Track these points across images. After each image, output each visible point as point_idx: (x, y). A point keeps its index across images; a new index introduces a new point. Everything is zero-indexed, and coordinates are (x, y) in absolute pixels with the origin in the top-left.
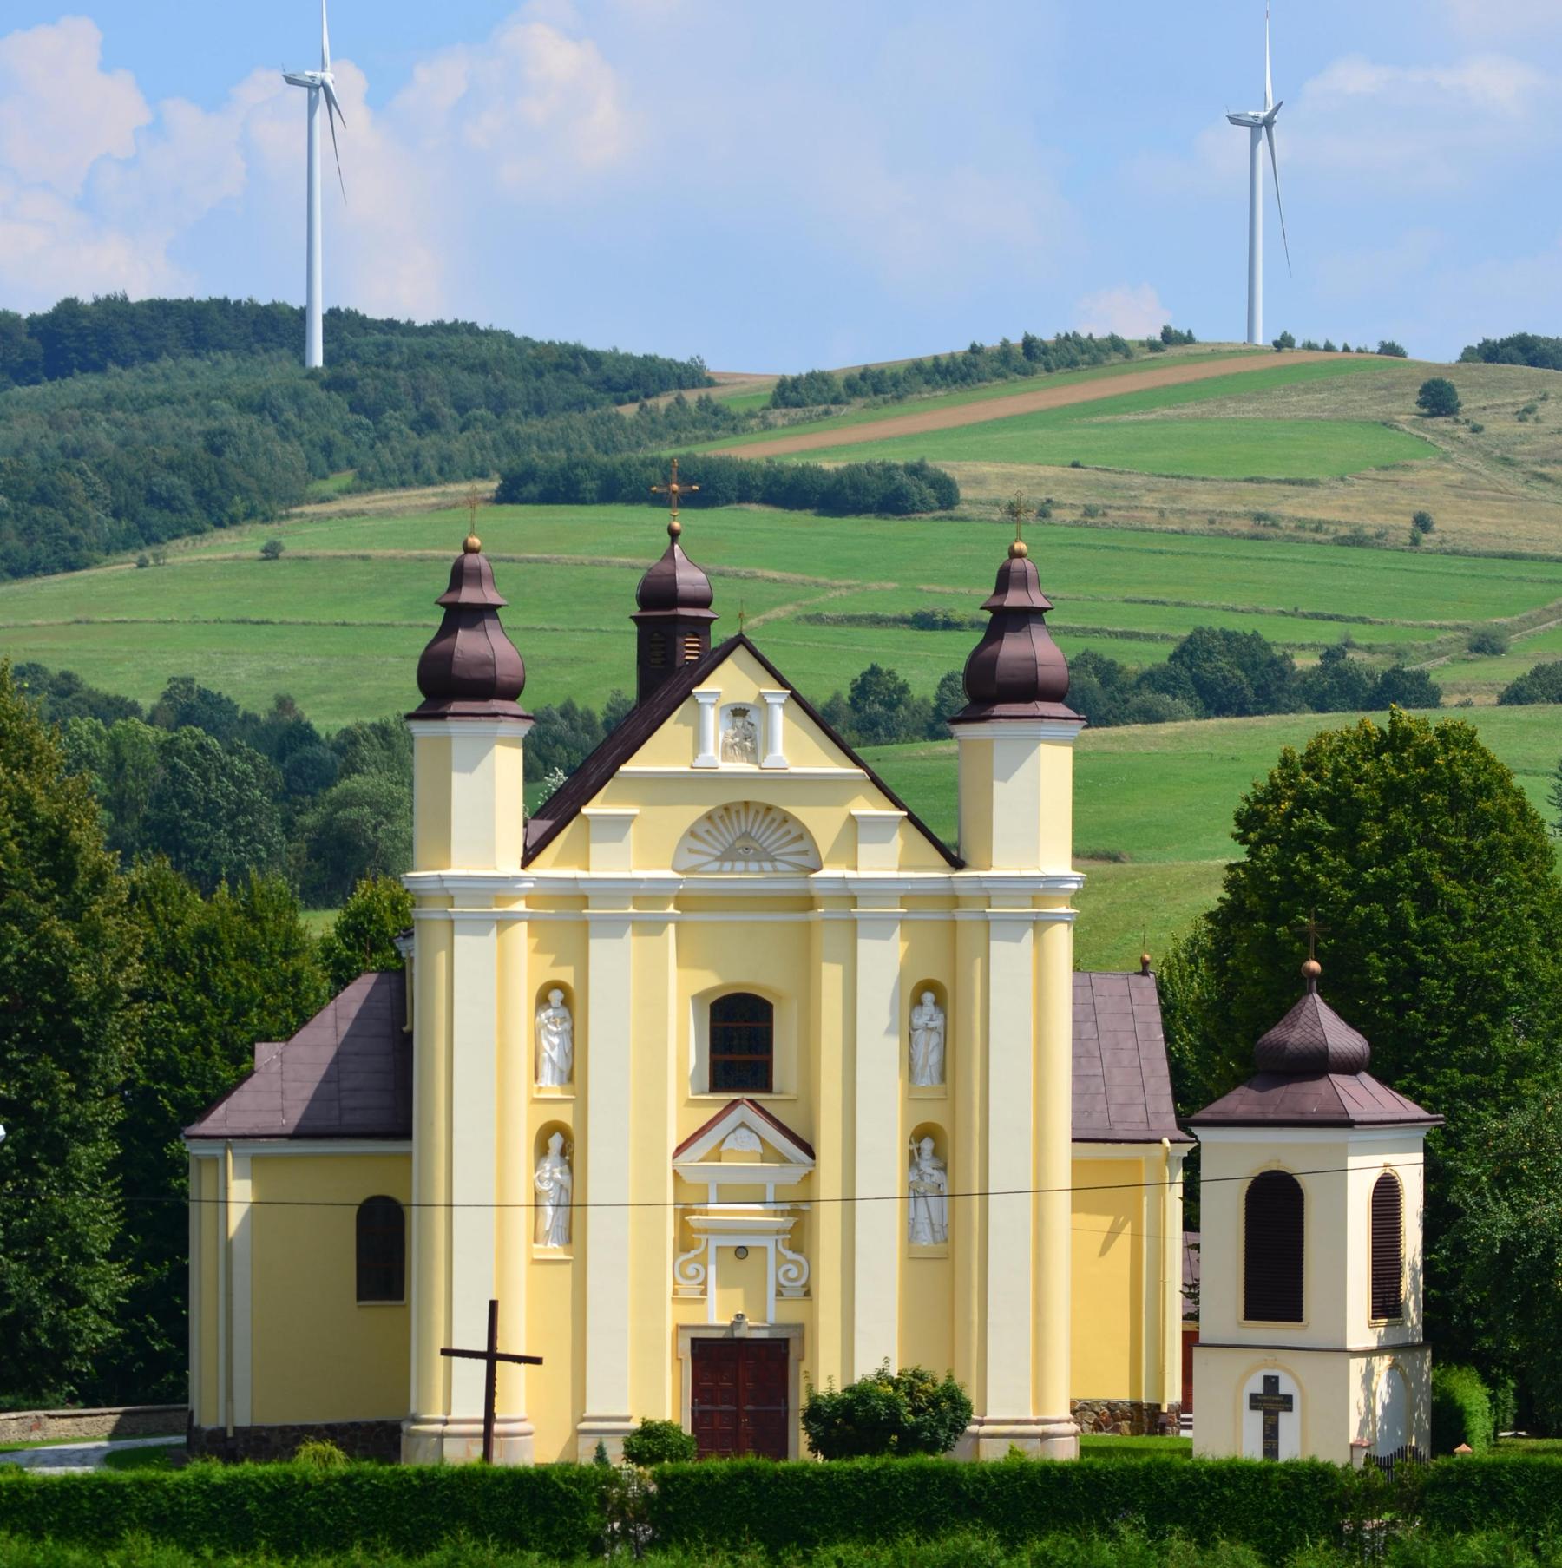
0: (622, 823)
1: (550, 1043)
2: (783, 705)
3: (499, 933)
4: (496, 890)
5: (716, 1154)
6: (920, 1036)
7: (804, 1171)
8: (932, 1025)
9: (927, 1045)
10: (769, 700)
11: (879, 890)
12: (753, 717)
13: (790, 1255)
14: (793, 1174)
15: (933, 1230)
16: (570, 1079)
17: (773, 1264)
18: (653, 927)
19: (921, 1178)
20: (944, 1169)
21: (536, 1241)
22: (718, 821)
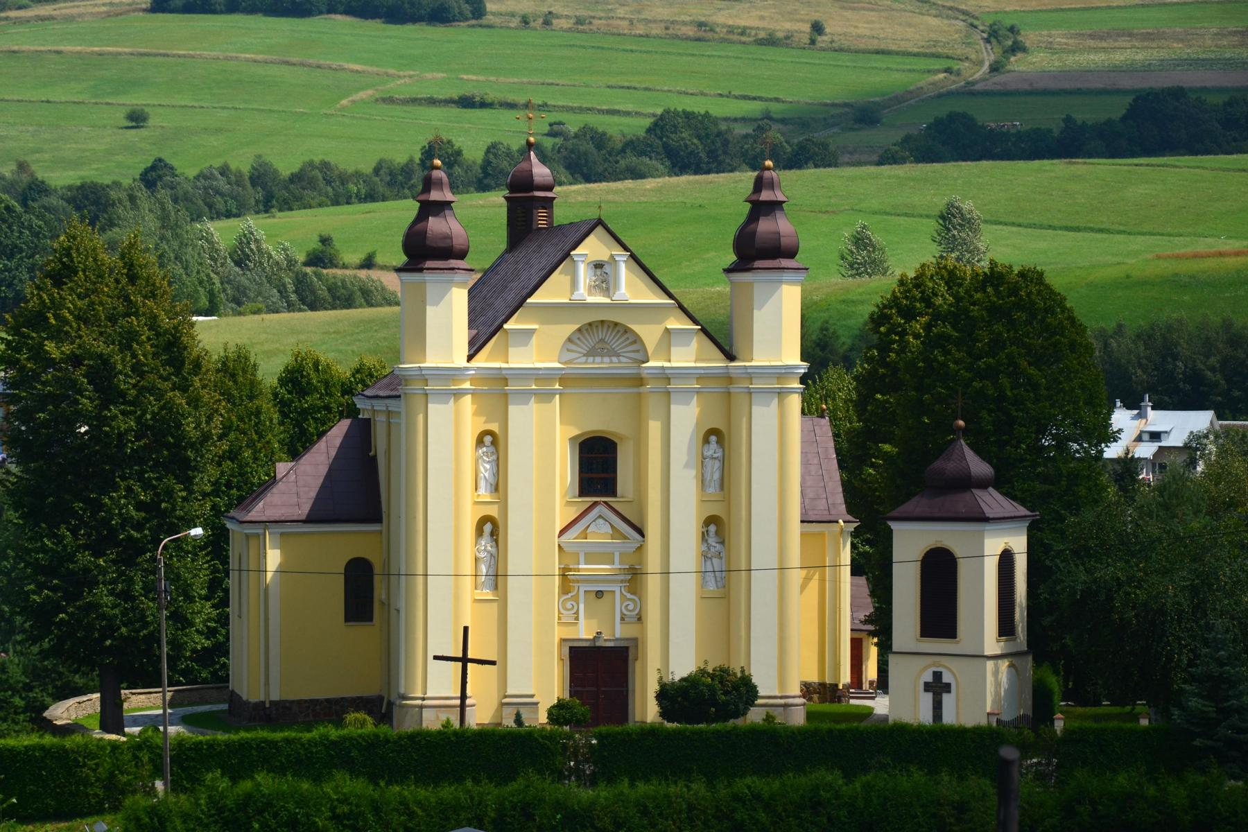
12: (607, 268)
13: (629, 596)
20: (722, 543)
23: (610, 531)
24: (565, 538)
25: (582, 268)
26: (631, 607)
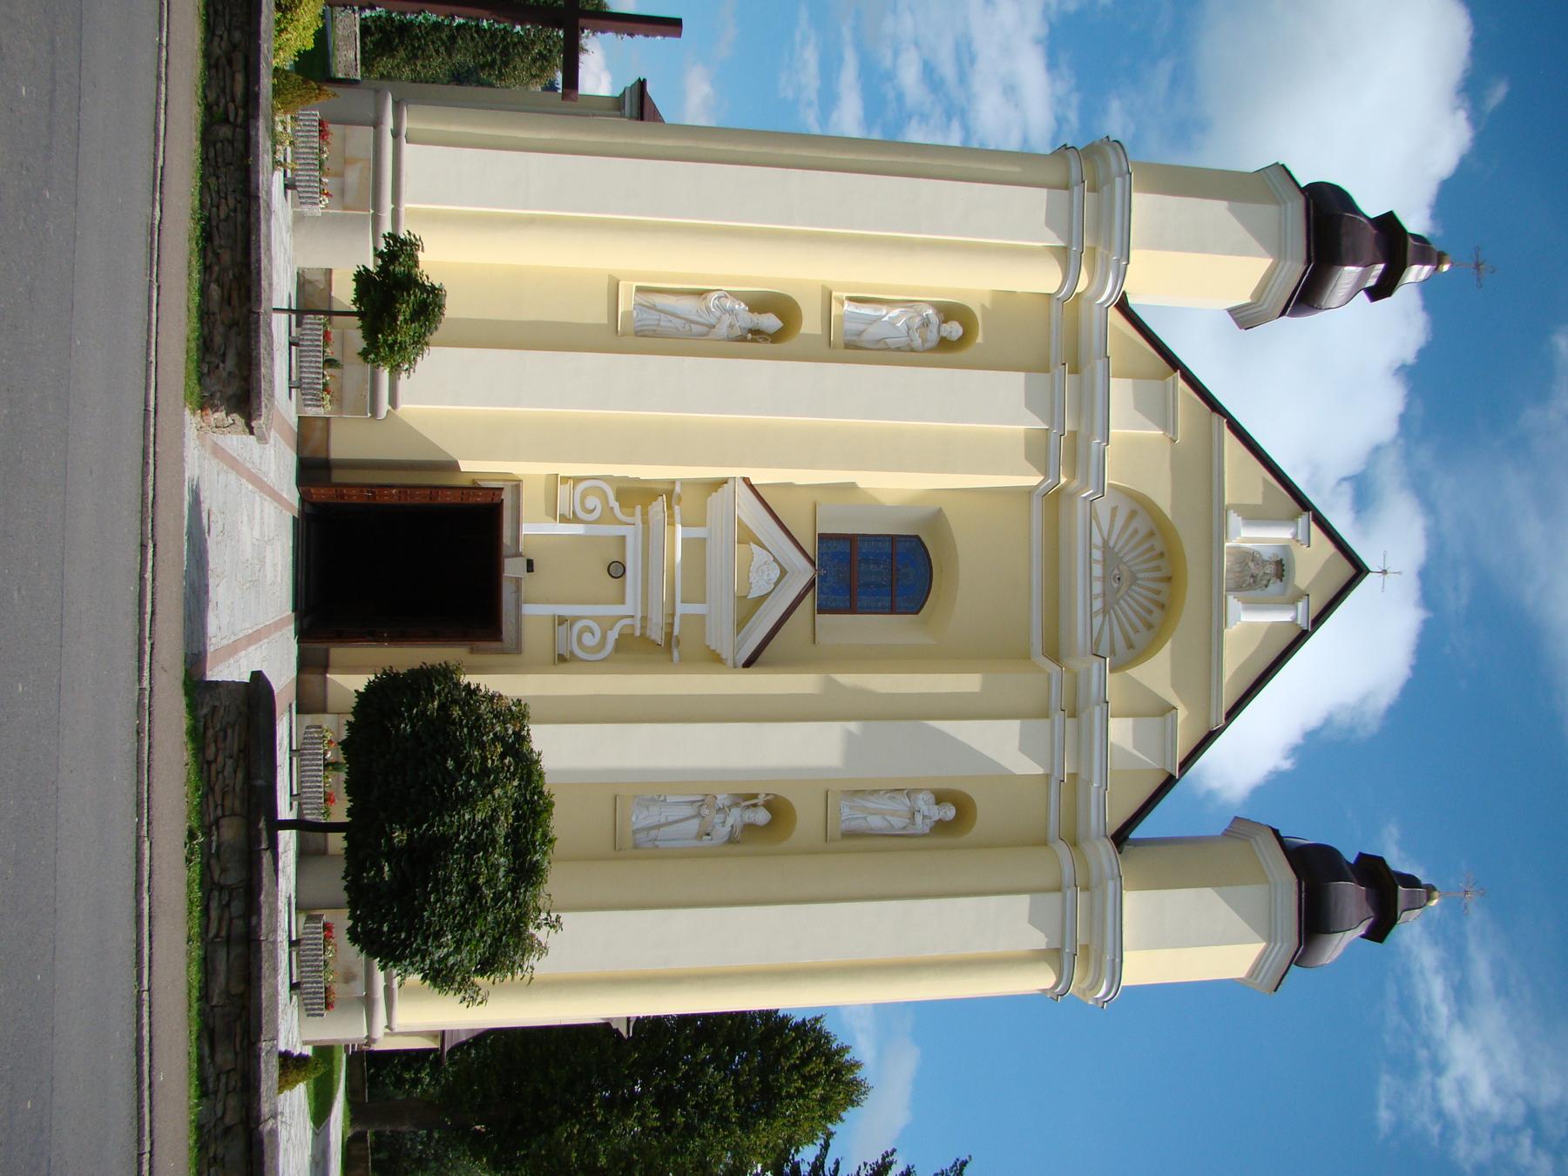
0: (1166, 420)
3: (1053, 250)
4: (1109, 247)
5: (747, 537)
6: (902, 804)
7: (726, 653)
8: (919, 818)
9: (894, 813)
10: (1301, 605)
12: (1275, 586)
13: (613, 636)
14: (721, 636)
16: (849, 346)
17: (599, 615)
18: (1039, 452)
20: (731, 840)
21: (639, 290)
22: (1146, 546)
24: (742, 490)
25: (1283, 534)
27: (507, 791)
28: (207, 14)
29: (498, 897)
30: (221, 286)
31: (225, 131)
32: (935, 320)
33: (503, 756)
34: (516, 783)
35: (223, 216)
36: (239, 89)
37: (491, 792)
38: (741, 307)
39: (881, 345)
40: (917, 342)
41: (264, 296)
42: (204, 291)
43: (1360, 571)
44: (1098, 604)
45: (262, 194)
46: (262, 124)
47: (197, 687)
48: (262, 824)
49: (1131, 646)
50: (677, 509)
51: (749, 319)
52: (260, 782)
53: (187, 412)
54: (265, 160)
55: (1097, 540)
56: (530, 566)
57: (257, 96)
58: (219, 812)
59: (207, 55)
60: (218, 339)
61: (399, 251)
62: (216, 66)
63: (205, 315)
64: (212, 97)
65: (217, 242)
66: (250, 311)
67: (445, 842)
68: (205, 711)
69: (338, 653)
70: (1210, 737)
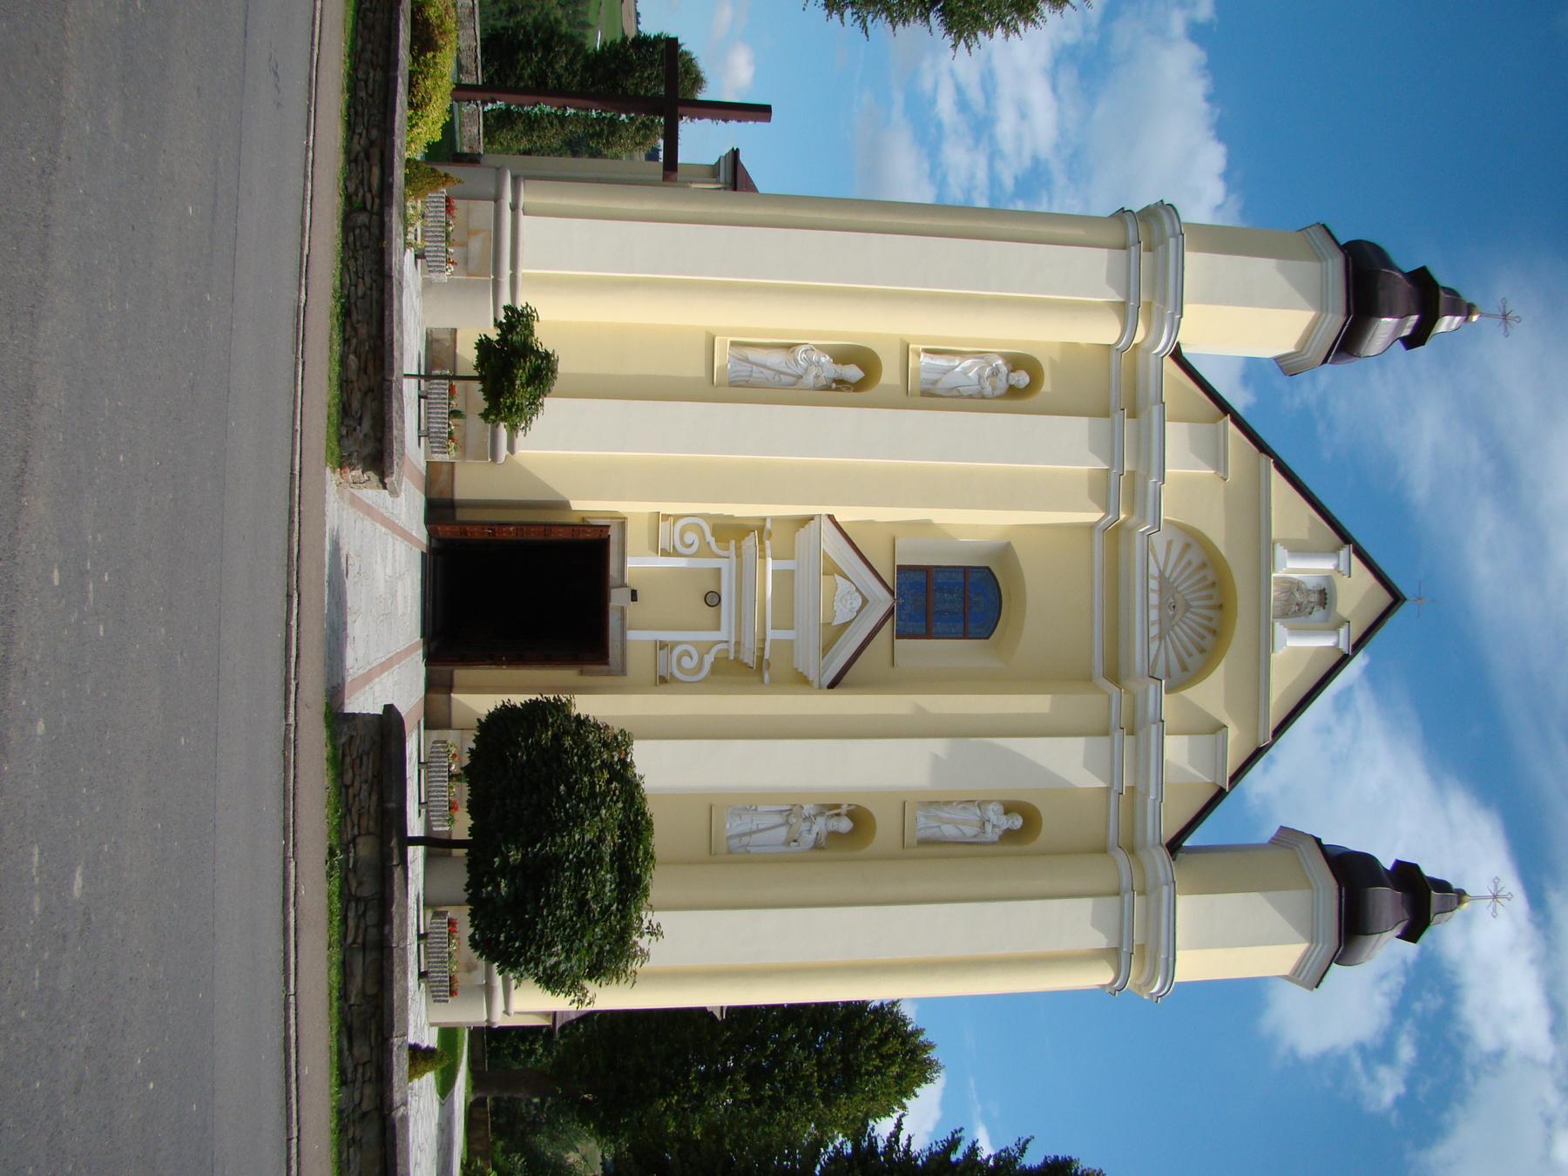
0: (1218, 460)
1: (970, 368)
2: (1336, 647)
4: (1164, 301)
5: (833, 569)
6: (973, 814)
7: (812, 675)
8: (989, 828)
10: (1343, 631)
11: (1148, 759)
12: (1318, 614)
13: (709, 659)
14: (808, 660)
15: (744, 834)
17: (696, 641)
18: (1103, 491)
19: (806, 819)
20: (817, 846)
21: (733, 344)
22: (1197, 577)
23: (838, 621)
24: (827, 526)
25: (1326, 565)
26: (686, 660)
27: (611, 813)
28: (349, 115)
29: (605, 911)
30: (358, 357)
31: (362, 218)
32: (1004, 369)
33: (609, 782)
34: (620, 805)
35: (360, 293)
36: (375, 181)
37: (599, 814)
38: (825, 359)
39: (955, 393)
40: (988, 390)
41: (396, 366)
42: (343, 362)
43: (1397, 598)
44: (1154, 631)
45: (395, 274)
46: (395, 211)
47: (336, 718)
48: (394, 843)
49: (1184, 668)
50: (768, 543)
51: (830, 369)
52: (392, 805)
53: (328, 470)
54: (398, 242)
55: (1153, 570)
56: (634, 596)
57: (391, 186)
58: (356, 831)
59: (348, 151)
60: (355, 405)
61: (517, 322)
62: (356, 161)
63: (344, 384)
64: (352, 189)
65: (354, 317)
66: (384, 379)
67: (556, 862)
68: (344, 740)
69: (462, 674)
70: (1258, 753)
